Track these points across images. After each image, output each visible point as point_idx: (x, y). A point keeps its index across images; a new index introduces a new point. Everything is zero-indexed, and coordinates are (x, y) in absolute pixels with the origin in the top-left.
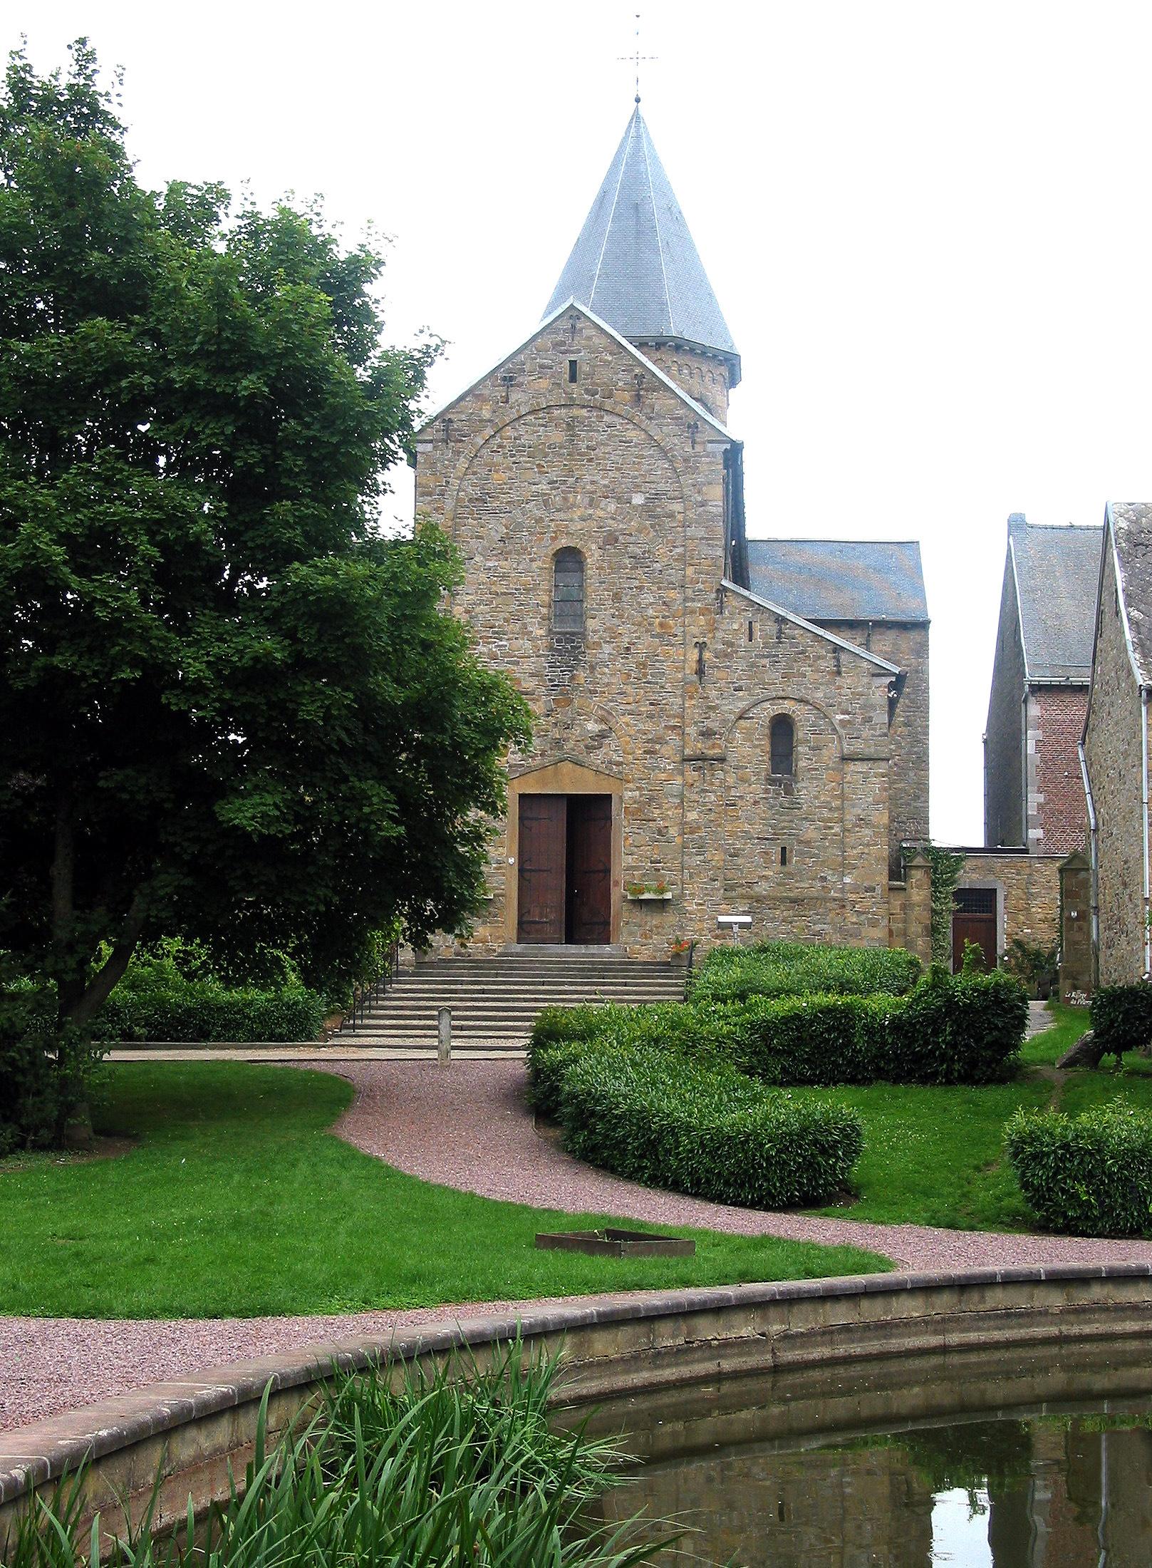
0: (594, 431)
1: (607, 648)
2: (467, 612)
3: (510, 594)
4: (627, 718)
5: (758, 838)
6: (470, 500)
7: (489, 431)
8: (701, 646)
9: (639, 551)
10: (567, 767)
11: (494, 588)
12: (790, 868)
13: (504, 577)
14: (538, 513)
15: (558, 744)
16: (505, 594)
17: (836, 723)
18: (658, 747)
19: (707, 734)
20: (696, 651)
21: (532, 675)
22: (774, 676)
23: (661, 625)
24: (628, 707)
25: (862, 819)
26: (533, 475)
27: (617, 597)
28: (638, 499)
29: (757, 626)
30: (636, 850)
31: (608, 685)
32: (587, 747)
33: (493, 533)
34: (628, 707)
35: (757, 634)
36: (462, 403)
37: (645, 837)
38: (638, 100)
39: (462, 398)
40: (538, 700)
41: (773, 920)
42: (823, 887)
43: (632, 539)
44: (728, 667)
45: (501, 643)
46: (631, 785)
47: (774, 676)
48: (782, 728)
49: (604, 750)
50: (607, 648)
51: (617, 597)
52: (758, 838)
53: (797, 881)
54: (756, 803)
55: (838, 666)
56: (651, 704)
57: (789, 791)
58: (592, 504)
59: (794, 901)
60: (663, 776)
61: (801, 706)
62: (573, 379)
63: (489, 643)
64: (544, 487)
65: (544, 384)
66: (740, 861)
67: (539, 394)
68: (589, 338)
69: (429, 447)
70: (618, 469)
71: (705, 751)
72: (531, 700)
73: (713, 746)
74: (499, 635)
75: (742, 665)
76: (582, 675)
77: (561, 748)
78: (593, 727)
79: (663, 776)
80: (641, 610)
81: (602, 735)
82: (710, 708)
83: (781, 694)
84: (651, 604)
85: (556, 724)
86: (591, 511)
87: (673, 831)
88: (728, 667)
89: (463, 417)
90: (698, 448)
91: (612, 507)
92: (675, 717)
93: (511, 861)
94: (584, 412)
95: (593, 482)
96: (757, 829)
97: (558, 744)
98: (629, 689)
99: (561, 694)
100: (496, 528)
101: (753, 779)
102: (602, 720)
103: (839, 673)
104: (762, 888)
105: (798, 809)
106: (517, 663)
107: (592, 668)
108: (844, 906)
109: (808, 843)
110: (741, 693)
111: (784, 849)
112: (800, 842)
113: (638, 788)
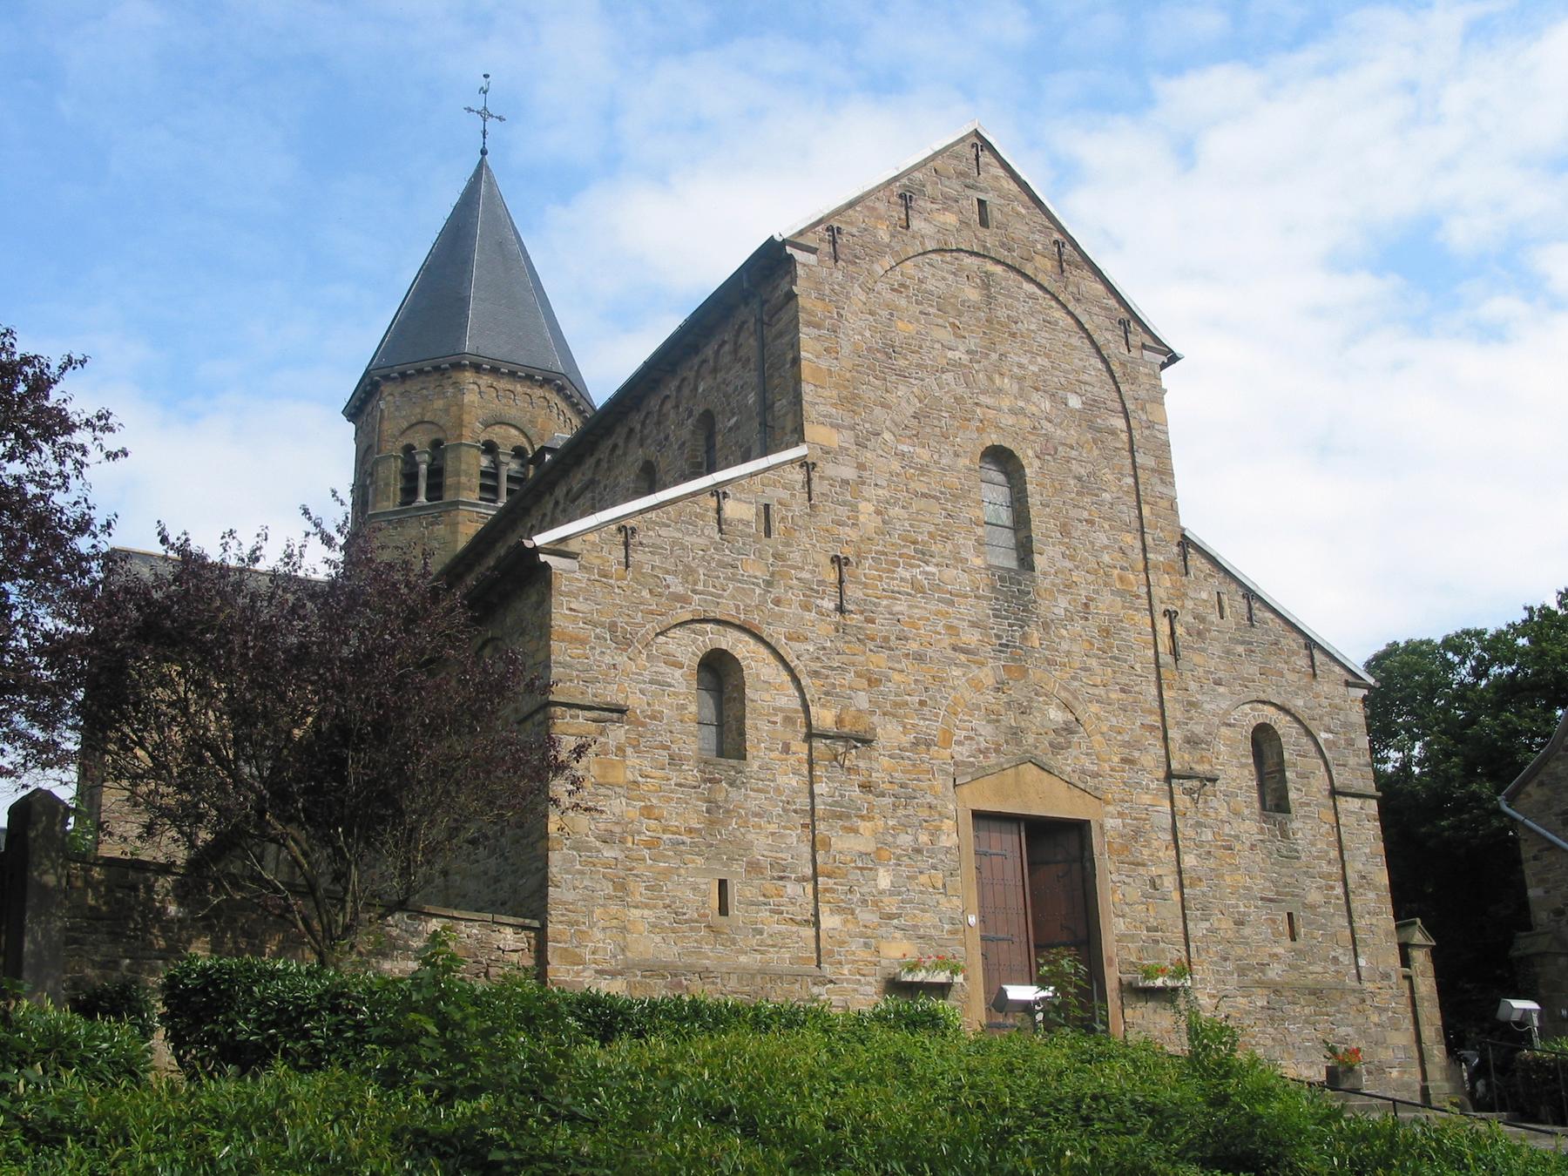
0: (1011, 297)
1: (1063, 602)
2: (878, 513)
3: (934, 497)
4: (1094, 708)
5: (1262, 899)
6: (869, 349)
7: (888, 261)
8: (1171, 615)
9: (1083, 471)
10: (1030, 771)
11: (912, 485)
12: (1299, 944)
13: (923, 470)
14: (960, 390)
15: (1015, 734)
16: (924, 495)
17: (1321, 742)
18: (1136, 754)
19: (1192, 742)
20: (1166, 621)
21: (974, 625)
22: (1251, 670)
23: (1121, 579)
24: (1096, 691)
25: (1364, 877)
26: (945, 335)
27: (1065, 531)
28: (1075, 402)
29: (1225, 598)
30: (1127, 909)
31: (1068, 653)
32: (1051, 744)
33: (904, 404)
34: (1096, 691)
35: (1227, 611)
36: (851, 212)
37: (1134, 893)
38: (484, 152)
39: (851, 205)
40: (983, 664)
41: (1294, 1019)
42: (1337, 972)
43: (1074, 453)
44: (1204, 650)
45: (927, 569)
46: (1110, 808)
47: (1251, 670)
48: (1264, 739)
49: (1073, 751)
50: (1063, 602)
51: (1065, 531)
52: (1262, 899)
53: (1310, 963)
54: (1253, 847)
55: (1313, 666)
56: (1123, 691)
57: (1284, 835)
58: (1021, 394)
59: (1313, 992)
60: (1147, 799)
61: (1282, 715)
62: (984, 222)
63: (912, 566)
64: (959, 355)
65: (950, 219)
66: (1247, 931)
67: (942, 230)
68: (997, 178)
69: (812, 259)
70: (1048, 356)
71: (1194, 766)
72: (974, 662)
73: (1201, 760)
74: (924, 555)
75: (1216, 649)
76: (1035, 635)
77: (1019, 743)
78: (1056, 715)
79: (1147, 799)
80: (1096, 552)
81: (1068, 730)
82: (1191, 704)
83: (1263, 696)
84: (1106, 547)
85: (1008, 703)
86: (1021, 404)
87: (1169, 883)
88: (1204, 650)
89: (854, 231)
90: (1135, 353)
91: (1046, 405)
92: (1151, 712)
93: (972, 920)
94: (999, 269)
95: (1021, 366)
96: (1260, 885)
97: (1015, 734)
98: (1093, 663)
99: (1014, 660)
100: (905, 398)
101: (1246, 812)
102: (1067, 707)
103: (1315, 675)
104: (1275, 972)
105: (1298, 858)
106: (951, 603)
107: (1046, 626)
108: (1364, 1001)
109: (1312, 907)
110: (1221, 689)
111: (1290, 915)
112: (1305, 905)
113: (1121, 815)
